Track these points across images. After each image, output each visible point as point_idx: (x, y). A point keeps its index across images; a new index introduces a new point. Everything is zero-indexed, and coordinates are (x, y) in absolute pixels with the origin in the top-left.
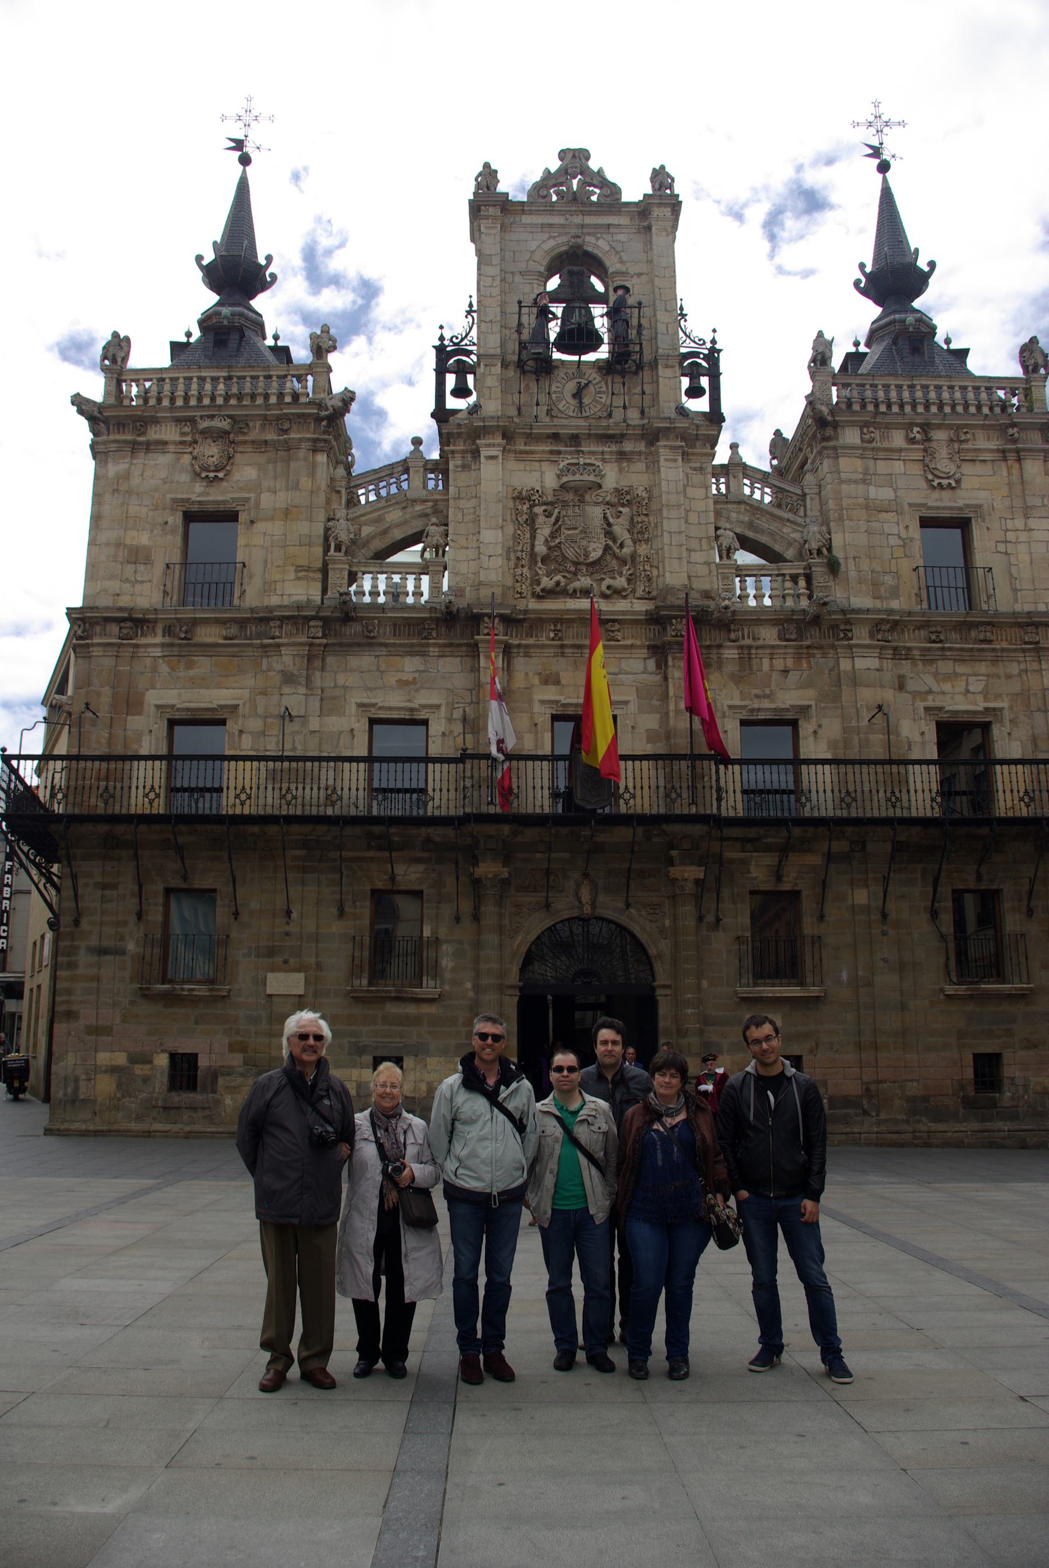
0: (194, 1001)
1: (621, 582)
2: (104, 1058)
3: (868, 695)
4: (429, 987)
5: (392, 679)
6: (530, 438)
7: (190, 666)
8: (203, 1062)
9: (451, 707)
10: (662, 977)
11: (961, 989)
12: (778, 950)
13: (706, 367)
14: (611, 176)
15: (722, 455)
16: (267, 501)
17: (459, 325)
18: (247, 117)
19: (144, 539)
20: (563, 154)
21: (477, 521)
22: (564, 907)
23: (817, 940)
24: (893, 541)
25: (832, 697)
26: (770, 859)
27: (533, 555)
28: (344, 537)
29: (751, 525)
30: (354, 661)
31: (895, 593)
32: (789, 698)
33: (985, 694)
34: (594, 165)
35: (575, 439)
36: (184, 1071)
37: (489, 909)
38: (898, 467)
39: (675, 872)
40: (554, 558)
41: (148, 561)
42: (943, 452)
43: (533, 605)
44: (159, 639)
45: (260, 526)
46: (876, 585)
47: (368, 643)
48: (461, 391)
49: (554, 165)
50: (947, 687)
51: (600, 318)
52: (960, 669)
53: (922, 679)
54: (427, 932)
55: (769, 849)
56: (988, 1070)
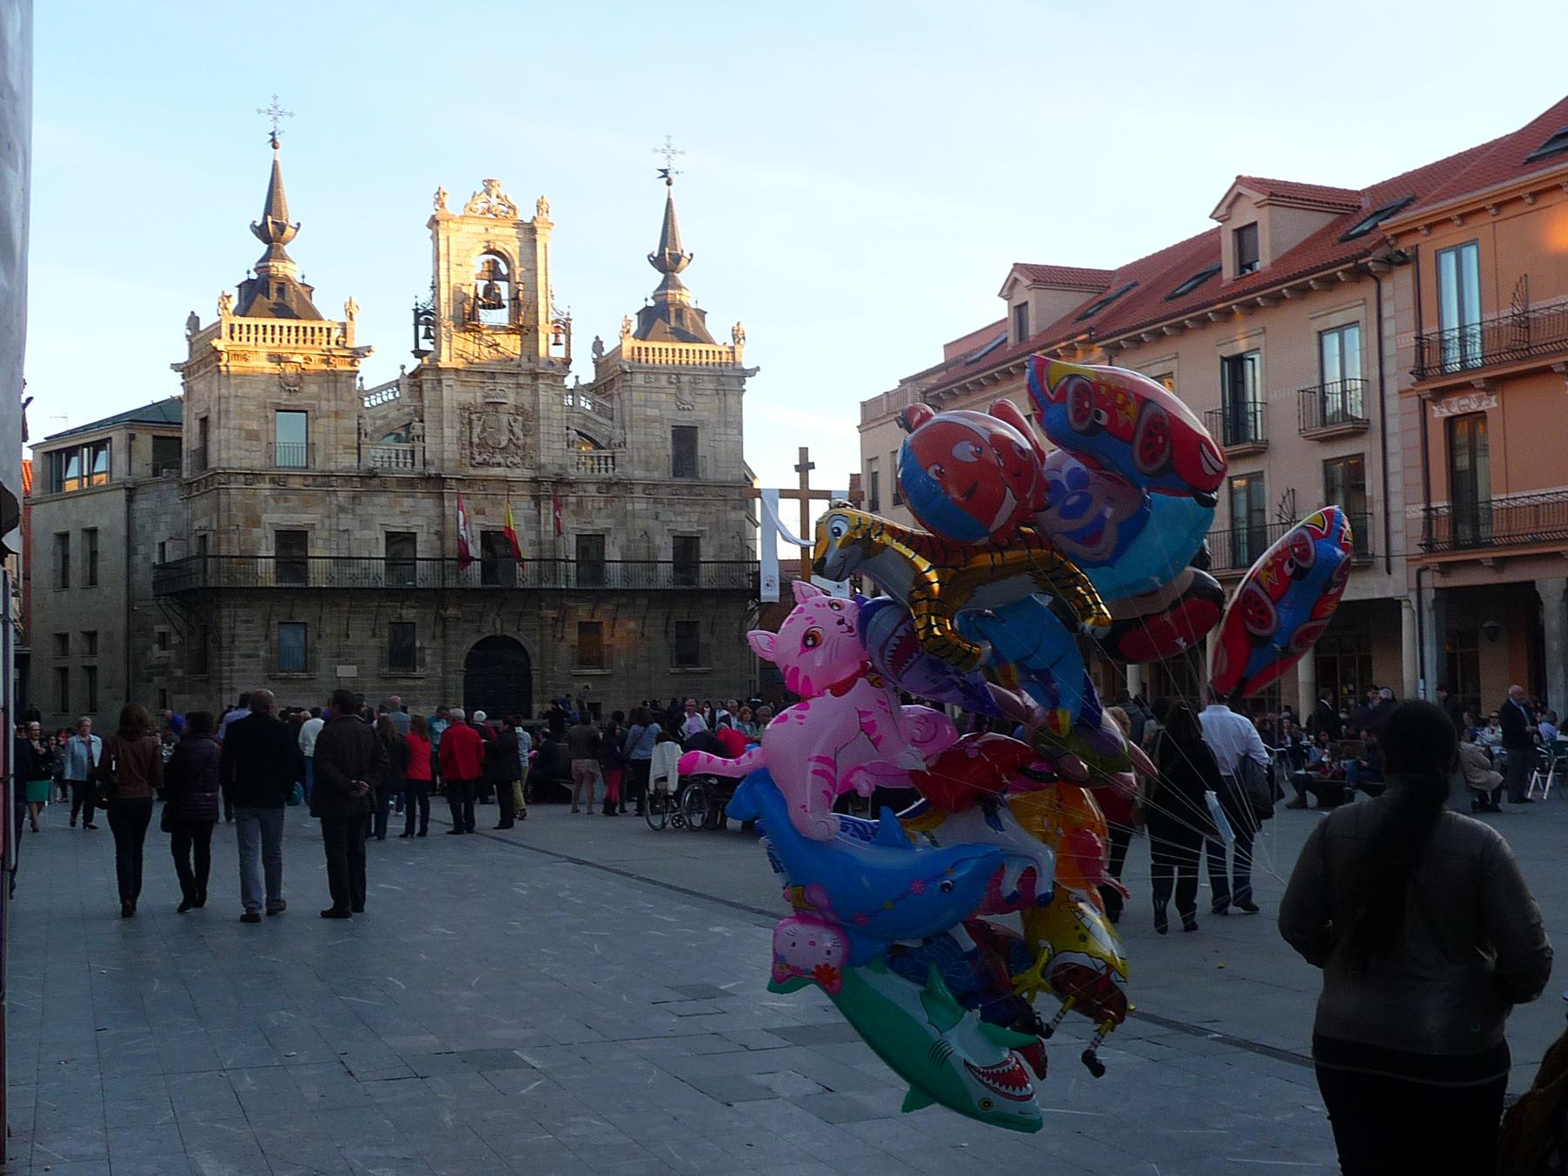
1: (517, 460)
3: (640, 523)
4: (419, 672)
7: (286, 500)
9: (429, 526)
10: (535, 665)
11: (677, 670)
16: (324, 405)
18: (275, 112)
19: (254, 426)
21: (441, 421)
22: (487, 631)
25: (622, 523)
27: (471, 443)
28: (369, 430)
29: (584, 426)
32: (601, 523)
33: (699, 523)
40: (483, 445)
42: (686, 389)
43: (472, 472)
44: (267, 486)
45: (322, 421)
46: (647, 463)
48: (427, 336)
51: (503, 288)
53: (667, 515)
54: (418, 644)
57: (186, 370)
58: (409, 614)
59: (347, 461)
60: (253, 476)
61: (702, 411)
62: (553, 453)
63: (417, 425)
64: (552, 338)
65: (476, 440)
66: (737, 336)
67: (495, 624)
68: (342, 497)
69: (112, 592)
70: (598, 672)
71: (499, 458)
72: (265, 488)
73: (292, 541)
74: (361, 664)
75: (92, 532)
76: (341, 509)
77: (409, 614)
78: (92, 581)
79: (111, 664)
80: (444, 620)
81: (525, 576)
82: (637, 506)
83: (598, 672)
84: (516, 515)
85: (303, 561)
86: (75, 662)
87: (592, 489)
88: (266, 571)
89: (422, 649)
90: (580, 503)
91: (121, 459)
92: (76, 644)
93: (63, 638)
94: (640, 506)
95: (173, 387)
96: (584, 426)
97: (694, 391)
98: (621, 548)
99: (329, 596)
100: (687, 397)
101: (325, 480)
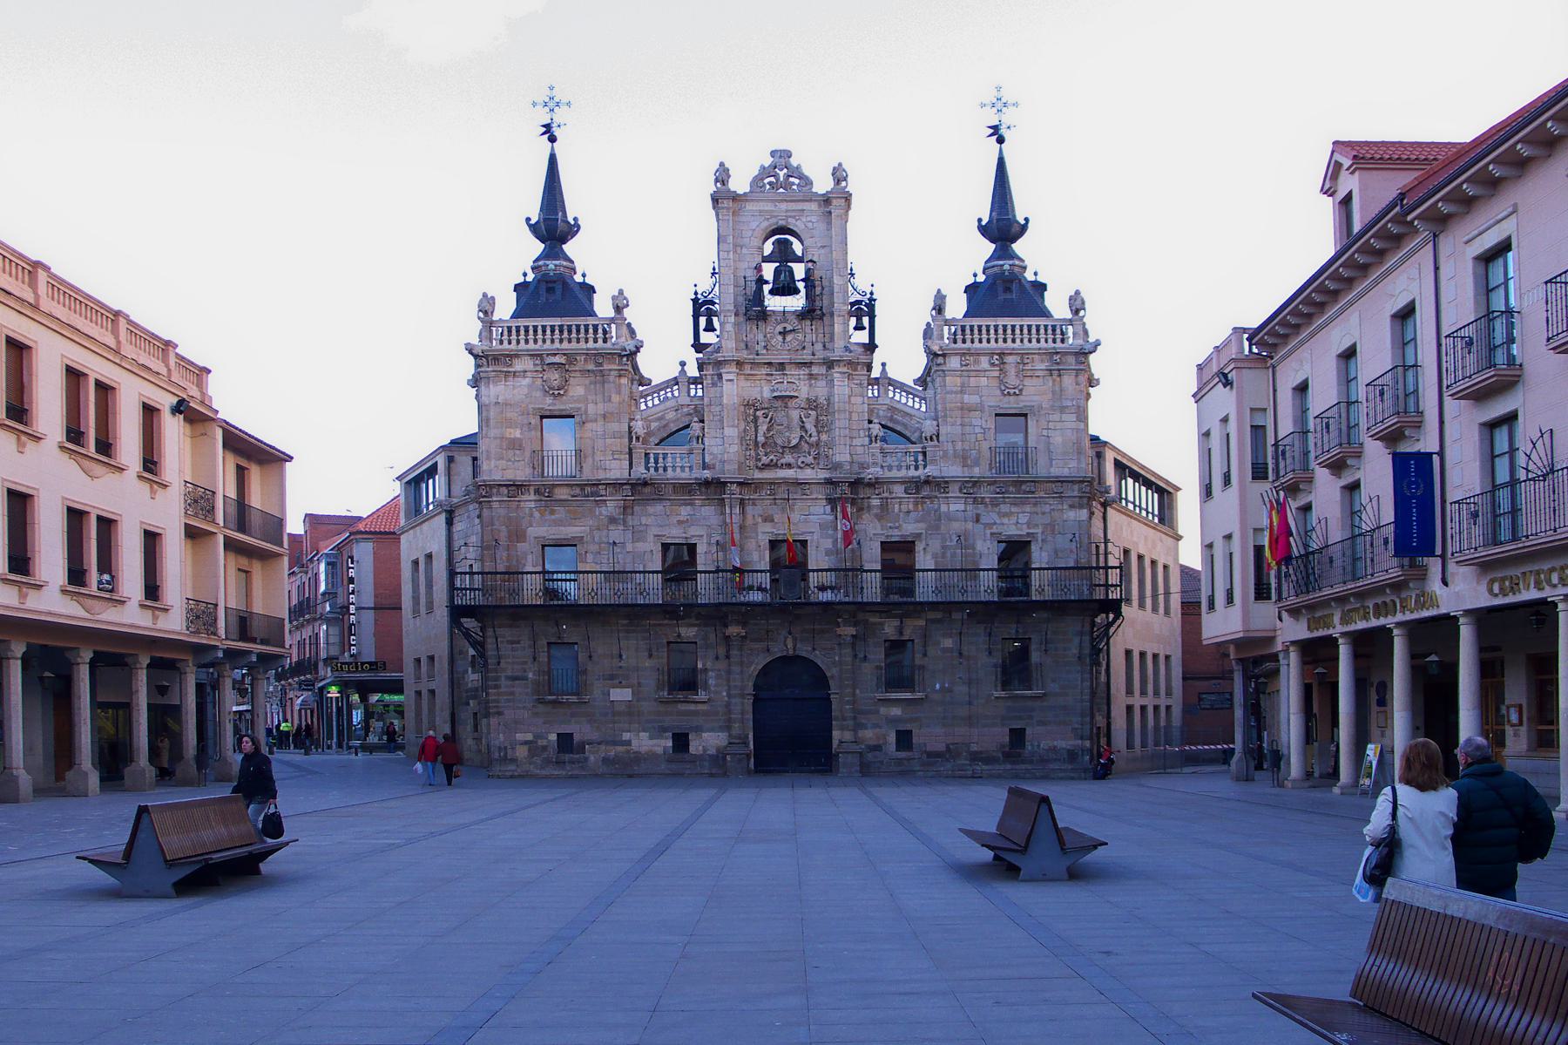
0: (568, 704)
1: (810, 459)
2: (520, 737)
3: (957, 526)
5: (674, 519)
6: (754, 364)
7: (553, 512)
8: (577, 738)
9: (709, 536)
11: (1003, 694)
13: (865, 310)
14: (806, 172)
15: (876, 373)
16: (591, 409)
17: (705, 285)
19: (517, 433)
20: (773, 154)
21: (721, 421)
22: (778, 651)
23: (922, 668)
24: (978, 430)
25: (935, 527)
26: (896, 623)
27: (756, 443)
30: (651, 509)
31: (977, 463)
32: (909, 528)
33: (1029, 524)
34: (794, 161)
35: (781, 366)
36: (565, 741)
37: (734, 652)
38: (984, 381)
39: (839, 631)
41: (521, 448)
43: (758, 475)
44: (532, 497)
47: (676, 610)
48: (710, 328)
49: (768, 161)
50: (1005, 520)
51: (799, 270)
52: (1014, 509)
53: (989, 516)
54: (700, 666)
55: (895, 617)
56: (1018, 736)
58: (688, 632)
59: (617, 470)
60: (517, 487)
61: (1036, 392)
62: (850, 448)
63: (696, 426)
64: (853, 321)
65: (761, 439)
66: (1077, 304)
67: (784, 645)
68: (611, 507)
70: (908, 695)
71: (788, 458)
72: (530, 497)
76: (612, 520)
80: (727, 638)
82: (953, 507)
83: (908, 695)
84: (812, 522)
87: (899, 490)
89: (705, 670)
90: (884, 506)
94: (956, 507)
96: (891, 419)
97: (1022, 374)
98: (935, 556)
100: (1012, 380)
101: (590, 490)
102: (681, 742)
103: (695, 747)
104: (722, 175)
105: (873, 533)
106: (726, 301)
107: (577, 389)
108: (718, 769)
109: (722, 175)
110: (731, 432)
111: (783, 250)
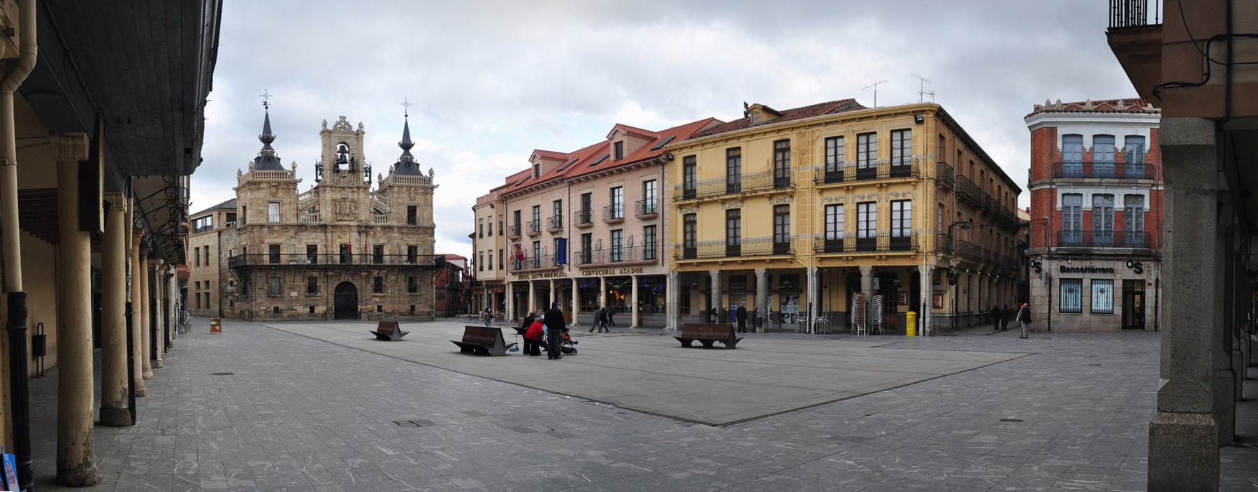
12: (378, 287)
17: (319, 160)
32: (382, 241)
53: (406, 238)
56: (413, 307)
57: (237, 190)
58: (315, 274)
59: (293, 221)
60: (262, 226)
61: (419, 200)
62: (365, 216)
66: (431, 172)
68: (291, 233)
69: (214, 267)
73: (275, 248)
74: (299, 292)
75: (207, 247)
77: (315, 274)
78: (207, 264)
79: (214, 291)
81: (356, 260)
85: (278, 255)
86: (202, 291)
88: (266, 260)
91: (216, 221)
92: (202, 285)
93: (198, 283)
95: (233, 195)
99: (287, 268)
101: (285, 227)
102: (312, 309)
103: (316, 311)
104: (325, 124)
105: (372, 242)
106: (328, 166)
107: (281, 194)
108: (324, 318)
109: (325, 124)
110: (329, 209)
111: (343, 148)
